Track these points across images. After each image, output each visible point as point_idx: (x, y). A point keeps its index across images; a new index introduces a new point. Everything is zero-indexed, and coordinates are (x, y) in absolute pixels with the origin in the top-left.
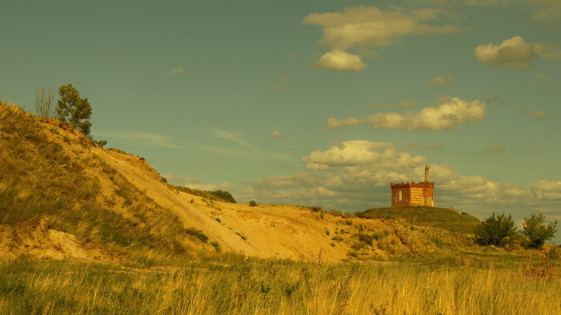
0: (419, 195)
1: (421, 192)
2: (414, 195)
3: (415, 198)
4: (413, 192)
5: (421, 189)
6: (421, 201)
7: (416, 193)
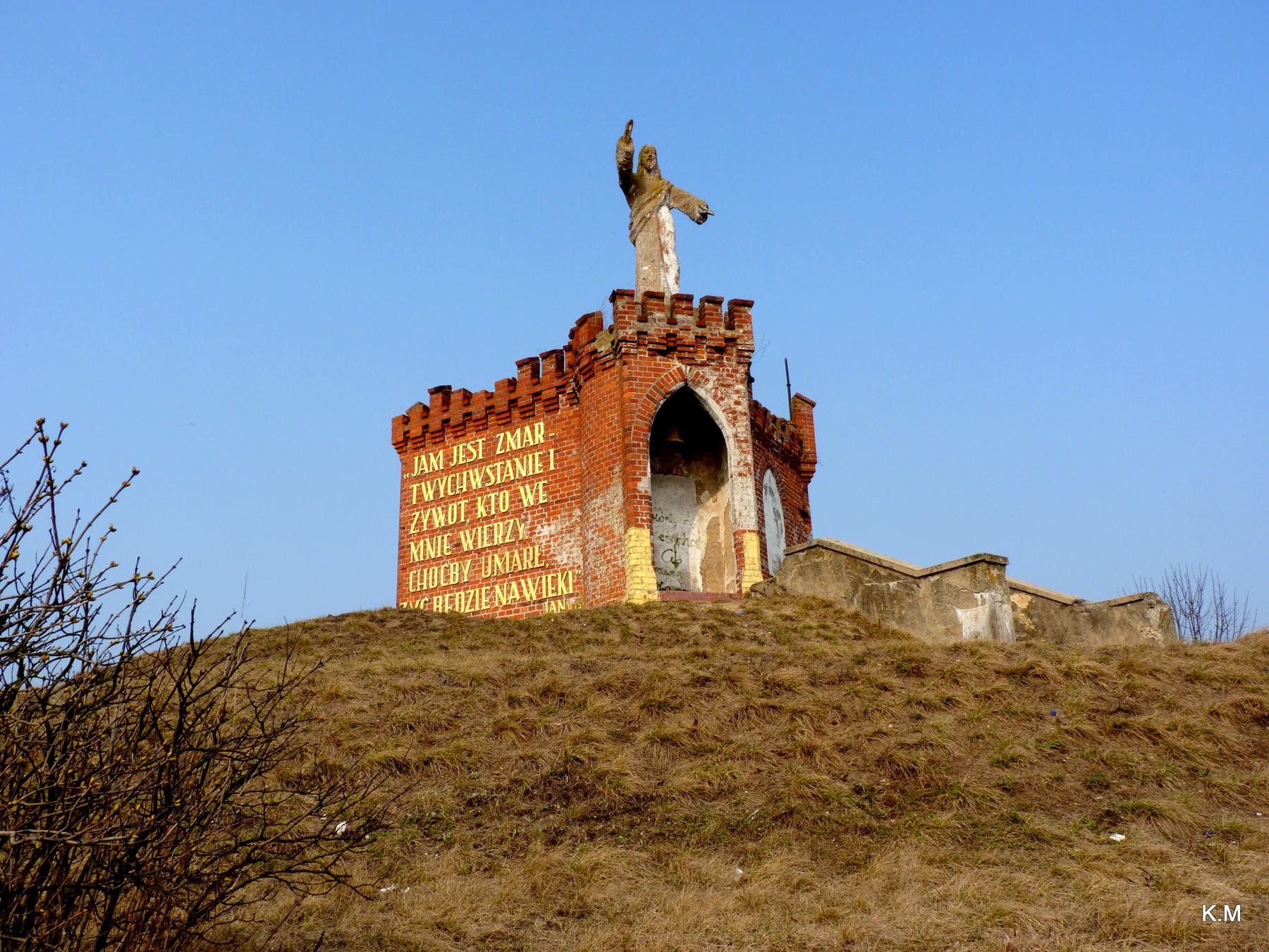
0: (517, 510)
1: (532, 465)
2: (445, 529)
3: (458, 552)
4: (428, 495)
5: (536, 432)
6: (547, 565)
7: (471, 495)
